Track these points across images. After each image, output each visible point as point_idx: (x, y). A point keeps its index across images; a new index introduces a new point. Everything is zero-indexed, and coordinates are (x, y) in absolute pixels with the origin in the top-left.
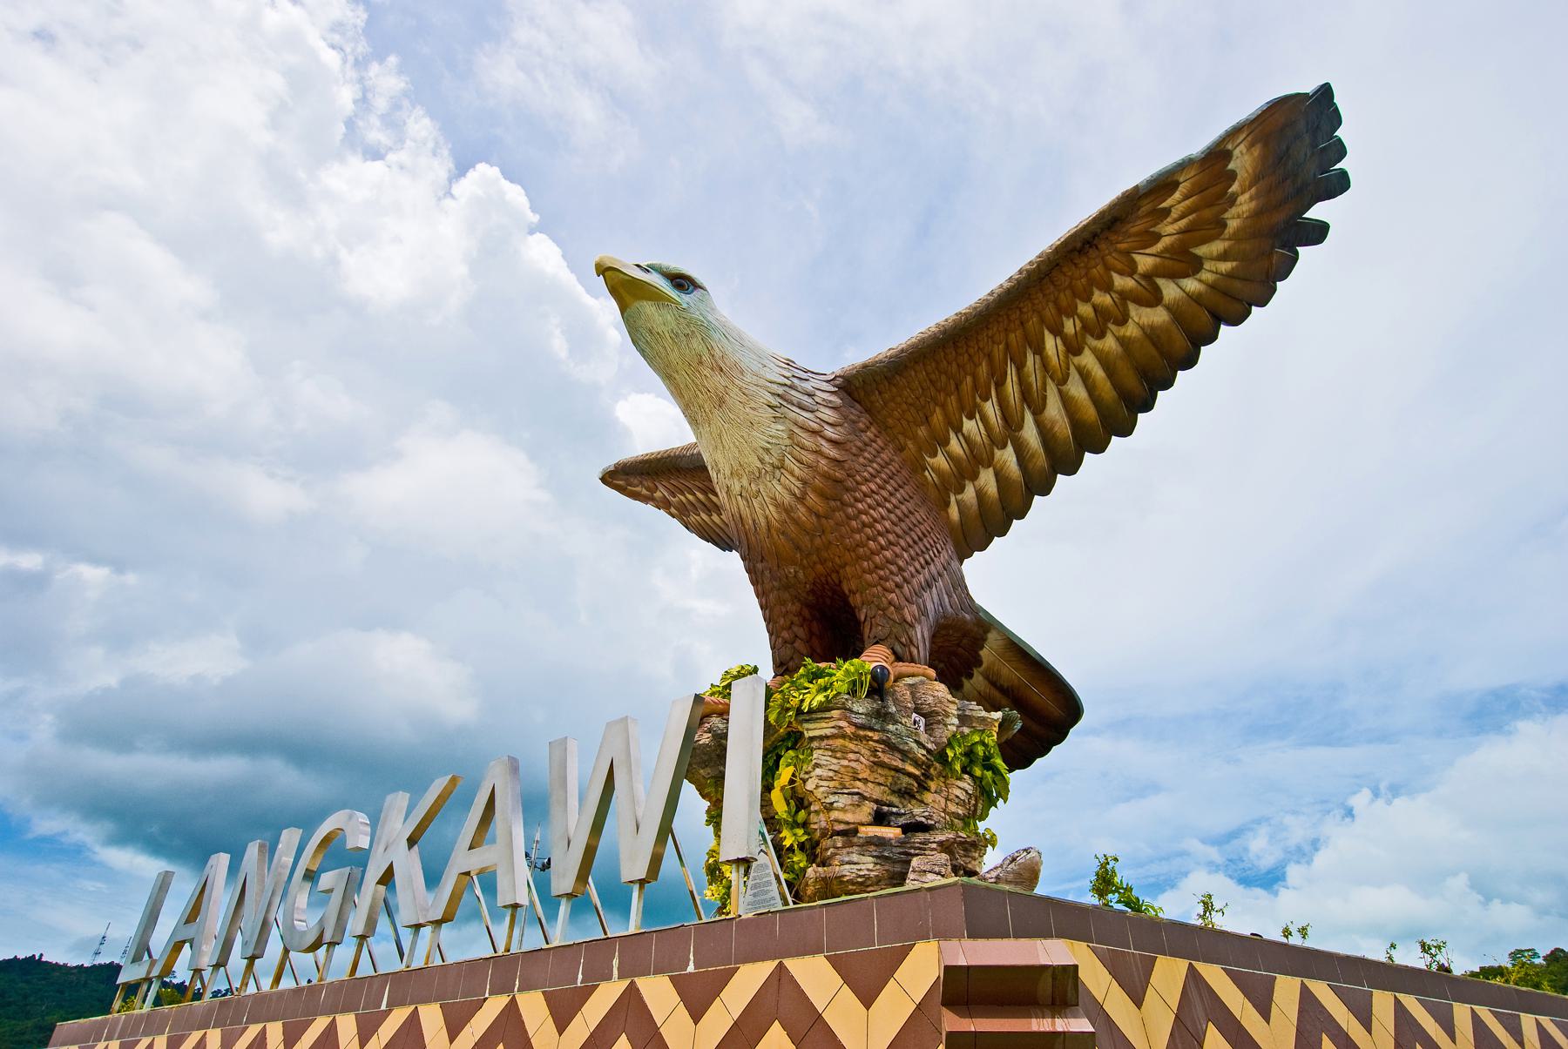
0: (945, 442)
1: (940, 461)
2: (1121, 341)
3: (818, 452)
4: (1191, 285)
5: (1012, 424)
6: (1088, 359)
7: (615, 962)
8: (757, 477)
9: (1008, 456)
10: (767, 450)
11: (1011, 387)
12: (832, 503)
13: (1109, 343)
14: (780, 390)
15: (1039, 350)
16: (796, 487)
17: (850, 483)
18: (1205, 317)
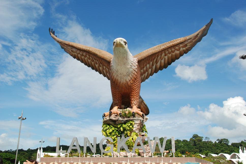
0: (144, 68)
1: (142, 71)
2: (172, 55)
3: (134, 74)
4: (184, 49)
5: (153, 65)
6: (166, 57)
7: (162, 159)
8: (124, 76)
9: (150, 70)
10: (128, 72)
11: (155, 60)
12: (134, 82)
13: (170, 55)
14: (132, 63)
15: (161, 55)
16: (130, 79)
17: (136, 79)
18: (183, 52)
